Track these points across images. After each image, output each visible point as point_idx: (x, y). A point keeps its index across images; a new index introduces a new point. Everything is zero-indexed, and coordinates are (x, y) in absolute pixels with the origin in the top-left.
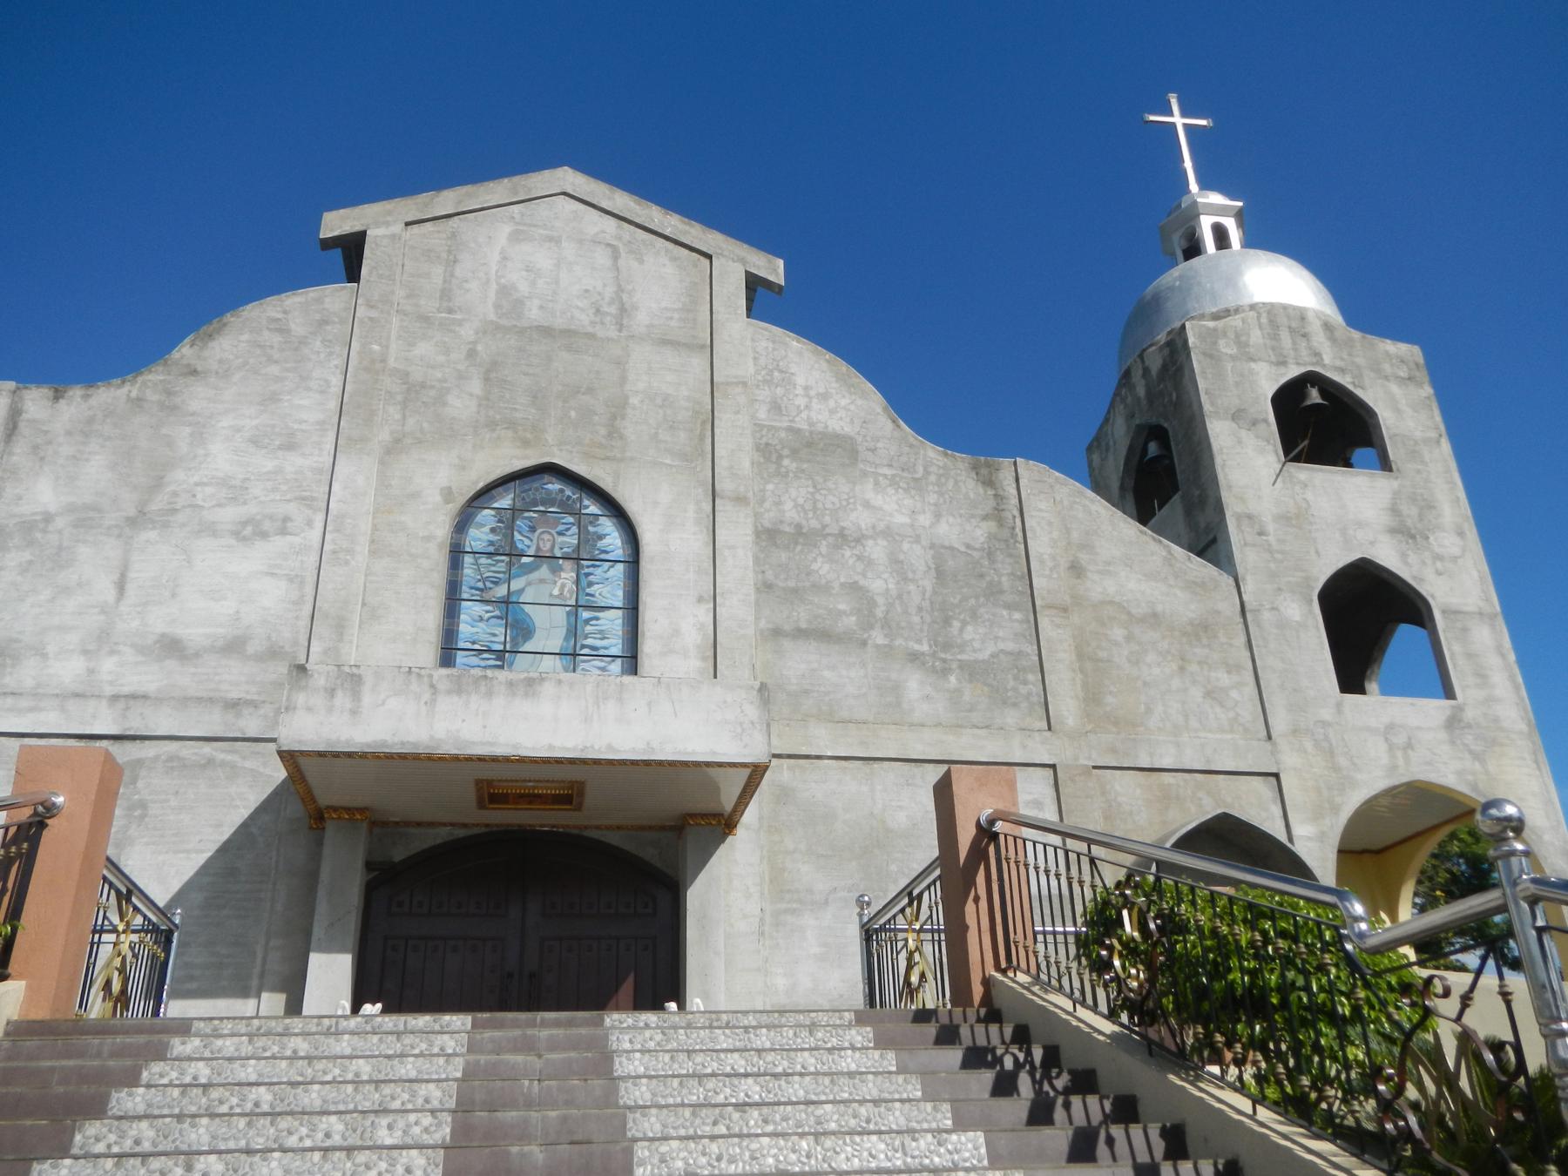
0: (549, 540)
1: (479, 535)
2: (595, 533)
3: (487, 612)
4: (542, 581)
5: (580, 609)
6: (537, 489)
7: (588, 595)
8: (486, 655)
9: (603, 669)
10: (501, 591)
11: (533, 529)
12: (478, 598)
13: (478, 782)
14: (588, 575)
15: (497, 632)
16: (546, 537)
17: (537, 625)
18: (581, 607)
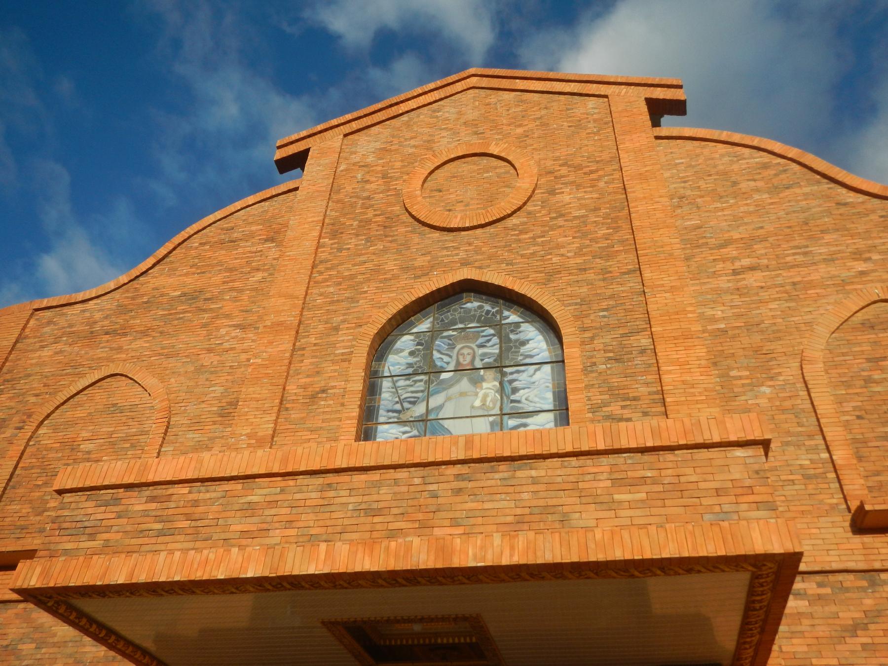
0: (468, 354)
2: (516, 341)
3: (404, 433)
4: (462, 394)
5: (506, 417)
6: (455, 310)
7: (513, 401)
10: (419, 410)
11: (452, 347)
12: (396, 420)
13: (330, 625)
14: (511, 382)
16: (466, 351)
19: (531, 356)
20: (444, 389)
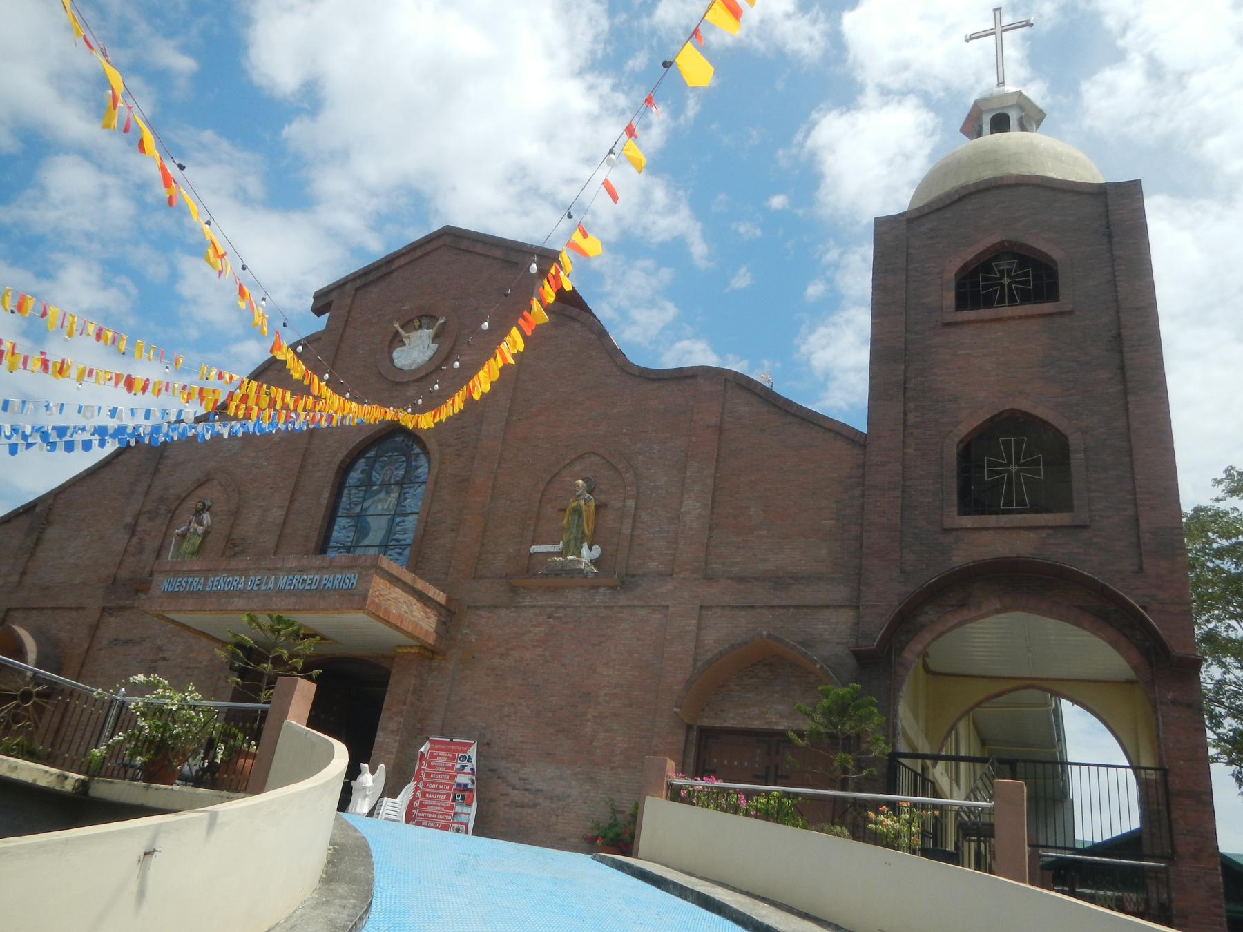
1: (355, 476)
4: (380, 500)
7: (403, 506)
8: (342, 550)
9: (400, 554)
10: (358, 509)
11: (383, 468)
12: (345, 515)
14: (405, 493)
15: (350, 535)
16: (388, 472)
17: (372, 528)
18: (400, 512)
19: (418, 477)
20: (373, 497)
